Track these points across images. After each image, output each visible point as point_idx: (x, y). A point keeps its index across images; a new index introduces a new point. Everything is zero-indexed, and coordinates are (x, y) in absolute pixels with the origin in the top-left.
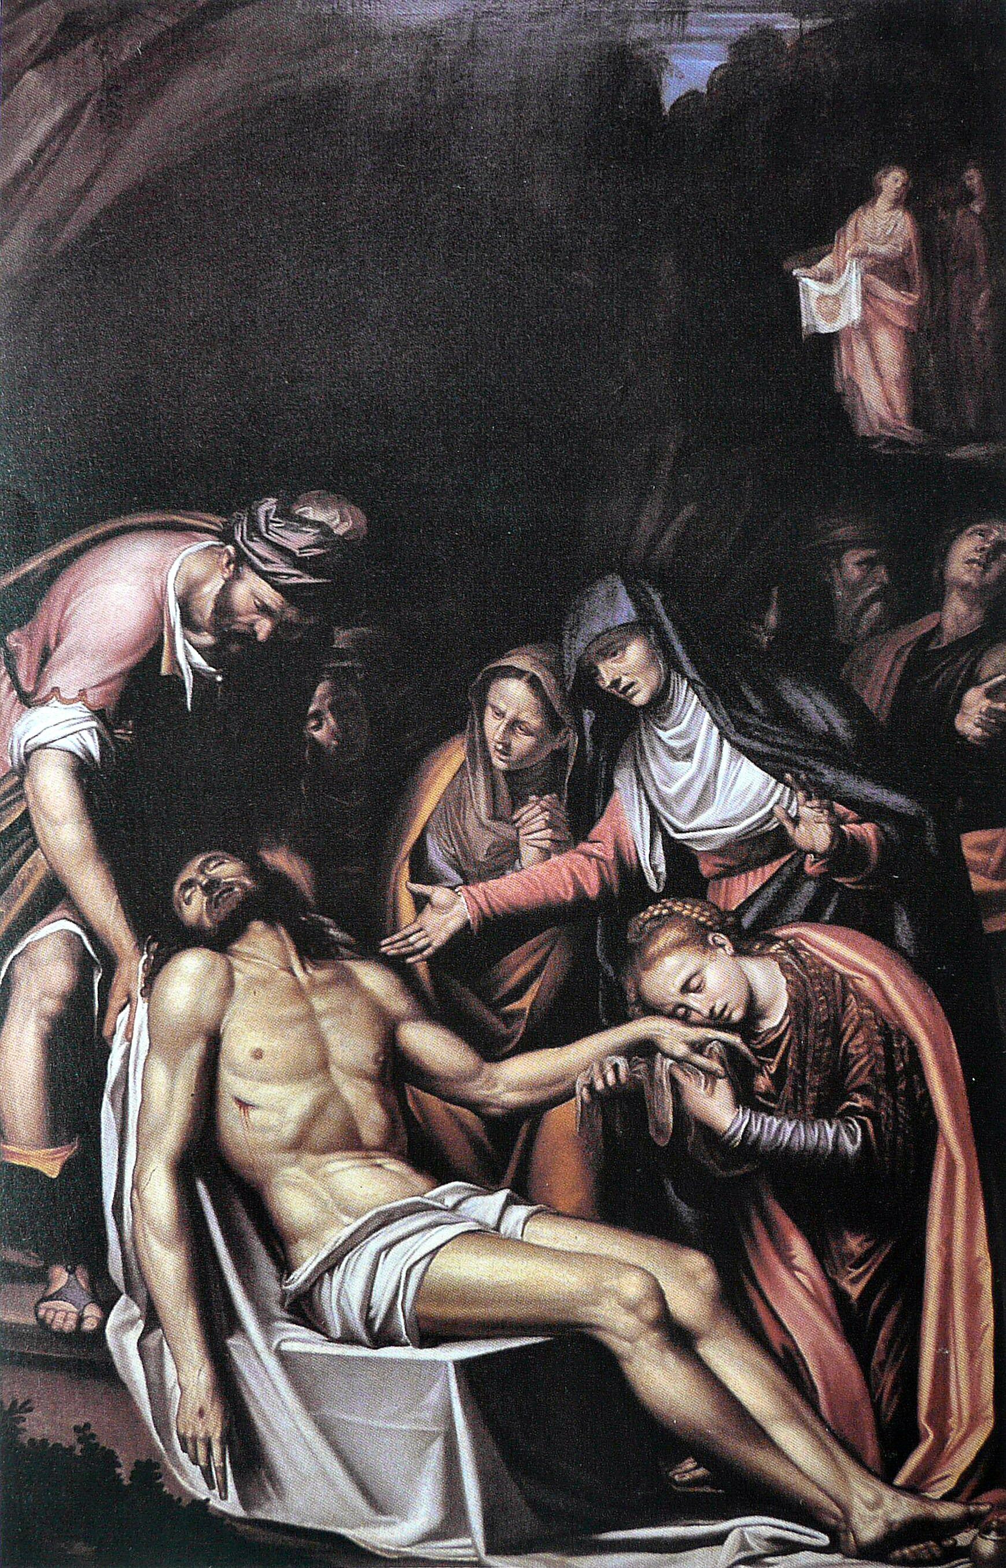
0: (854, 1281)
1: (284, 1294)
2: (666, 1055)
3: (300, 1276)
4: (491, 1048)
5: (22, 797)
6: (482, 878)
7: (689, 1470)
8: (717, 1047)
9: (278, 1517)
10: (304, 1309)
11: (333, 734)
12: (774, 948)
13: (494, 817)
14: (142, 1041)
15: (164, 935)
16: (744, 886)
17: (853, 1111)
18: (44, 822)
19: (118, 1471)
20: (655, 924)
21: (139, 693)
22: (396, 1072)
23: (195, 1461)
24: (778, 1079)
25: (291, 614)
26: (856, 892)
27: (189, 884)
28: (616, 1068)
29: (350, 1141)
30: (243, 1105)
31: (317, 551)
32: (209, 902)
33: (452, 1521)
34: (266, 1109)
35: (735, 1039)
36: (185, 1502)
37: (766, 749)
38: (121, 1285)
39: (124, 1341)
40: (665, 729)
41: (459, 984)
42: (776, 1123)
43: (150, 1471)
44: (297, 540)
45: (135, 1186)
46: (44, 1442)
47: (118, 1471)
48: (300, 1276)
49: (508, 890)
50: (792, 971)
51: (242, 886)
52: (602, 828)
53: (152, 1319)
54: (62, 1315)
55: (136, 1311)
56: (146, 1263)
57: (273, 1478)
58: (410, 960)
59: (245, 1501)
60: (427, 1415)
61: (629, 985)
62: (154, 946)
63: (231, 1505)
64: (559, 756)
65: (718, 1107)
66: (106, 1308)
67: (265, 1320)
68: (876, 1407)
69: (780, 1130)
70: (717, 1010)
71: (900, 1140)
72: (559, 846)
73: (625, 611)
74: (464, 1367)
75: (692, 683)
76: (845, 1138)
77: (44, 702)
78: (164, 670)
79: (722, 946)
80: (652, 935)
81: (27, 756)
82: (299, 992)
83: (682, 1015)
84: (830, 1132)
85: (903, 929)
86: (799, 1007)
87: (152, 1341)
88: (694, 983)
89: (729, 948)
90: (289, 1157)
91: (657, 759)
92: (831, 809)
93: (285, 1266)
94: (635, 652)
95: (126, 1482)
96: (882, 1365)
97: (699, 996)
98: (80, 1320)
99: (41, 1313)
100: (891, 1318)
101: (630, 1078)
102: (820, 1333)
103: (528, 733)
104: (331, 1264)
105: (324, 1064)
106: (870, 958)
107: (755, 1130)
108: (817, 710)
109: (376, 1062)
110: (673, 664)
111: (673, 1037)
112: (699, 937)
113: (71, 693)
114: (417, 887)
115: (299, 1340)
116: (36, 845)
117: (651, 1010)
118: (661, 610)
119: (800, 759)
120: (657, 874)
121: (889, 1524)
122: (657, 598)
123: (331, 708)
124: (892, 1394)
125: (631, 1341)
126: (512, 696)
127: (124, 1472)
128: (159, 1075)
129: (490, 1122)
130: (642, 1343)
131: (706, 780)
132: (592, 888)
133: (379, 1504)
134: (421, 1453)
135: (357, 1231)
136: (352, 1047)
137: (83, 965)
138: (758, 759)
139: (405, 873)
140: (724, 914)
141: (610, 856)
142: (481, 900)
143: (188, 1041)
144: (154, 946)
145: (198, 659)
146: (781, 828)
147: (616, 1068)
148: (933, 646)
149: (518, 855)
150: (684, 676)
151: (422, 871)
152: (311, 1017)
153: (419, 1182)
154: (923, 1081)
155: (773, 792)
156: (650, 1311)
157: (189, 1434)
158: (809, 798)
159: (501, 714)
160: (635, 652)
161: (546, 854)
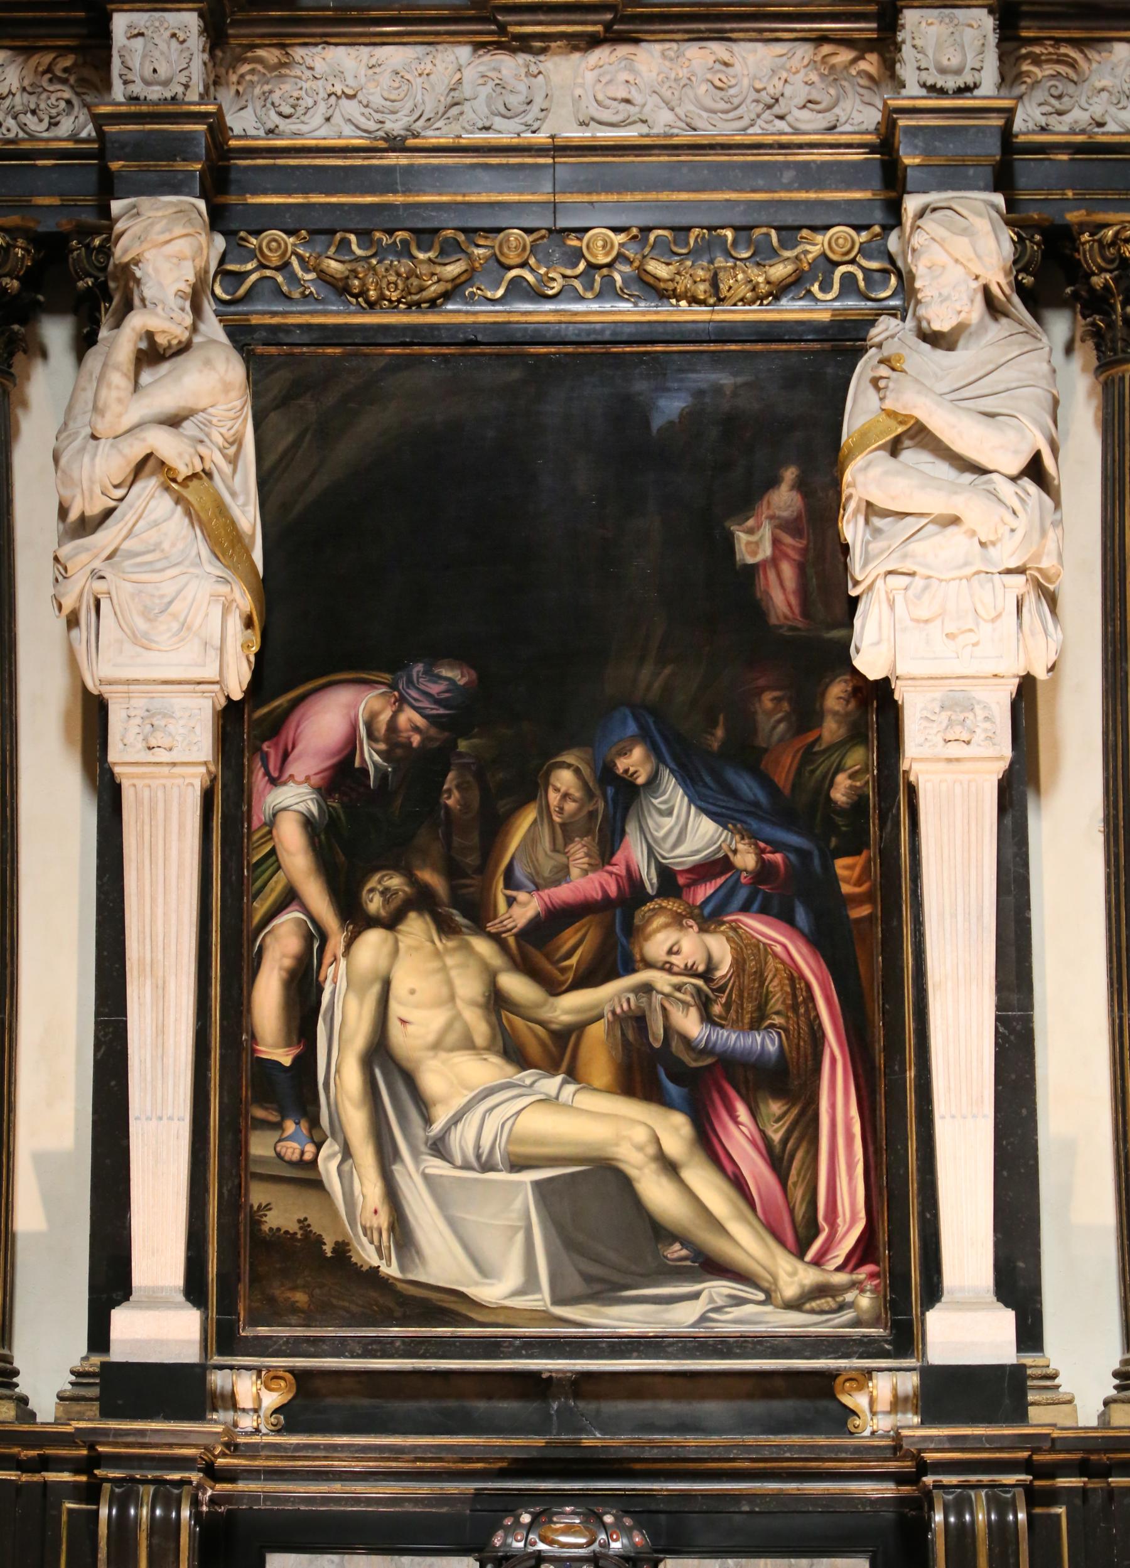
0: (776, 1131)
1: (427, 1138)
2: (658, 992)
3: (437, 1128)
4: (554, 989)
5: (272, 838)
6: (547, 886)
7: (676, 1251)
8: (689, 988)
9: (422, 1278)
10: (439, 1148)
11: (458, 802)
12: (723, 928)
13: (555, 850)
14: (342, 984)
15: (356, 919)
16: (704, 892)
17: (772, 1026)
18: (285, 854)
19: (324, 1247)
20: (651, 914)
21: (341, 776)
22: (496, 1002)
23: (372, 1242)
24: (727, 1006)
25: (433, 732)
26: (771, 894)
27: (372, 890)
28: (628, 1000)
29: (468, 1044)
30: (404, 1022)
31: (447, 695)
32: (384, 901)
33: (530, 1284)
34: (418, 1025)
35: (700, 982)
36: (364, 1269)
37: (719, 810)
38: (328, 1133)
39: (329, 1167)
40: (656, 798)
41: (533, 949)
42: (726, 1034)
43: (342, 1249)
44: (435, 689)
45: (338, 1071)
46: (279, 1229)
47: (324, 1247)
48: (437, 1128)
49: (563, 893)
50: (734, 942)
51: (404, 891)
52: (619, 857)
53: (347, 1153)
54: (292, 1150)
55: (336, 1148)
56: (343, 1118)
57: (419, 1252)
58: (504, 935)
59: (402, 1268)
60: (514, 1215)
61: (636, 951)
62: (351, 927)
63: (391, 1270)
64: (592, 815)
65: (690, 1024)
66: (319, 1146)
67: (416, 1154)
68: (791, 1211)
69: (730, 1038)
70: (689, 965)
71: (802, 1044)
72: (593, 867)
73: (632, 728)
74: (538, 1185)
75: (672, 771)
76: (768, 1041)
77: (285, 783)
78: (357, 764)
79: (691, 927)
80: (649, 921)
81: (275, 815)
82: (437, 954)
83: (667, 968)
84: (759, 1039)
85: (801, 916)
86: (739, 964)
87: (346, 1167)
88: (675, 949)
89: (696, 928)
90: (431, 1054)
91: (651, 815)
92: (757, 845)
93: (428, 1121)
94: (638, 753)
95: (329, 1255)
96: (795, 1184)
97: (678, 957)
98: (302, 1153)
99: (278, 1149)
100: (799, 1155)
101: (638, 1007)
102: (754, 1164)
103: (574, 801)
104: (456, 1120)
105: (452, 997)
106: (784, 935)
107: (713, 1038)
108: (747, 786)
109: (484, 996)
110: (660, 759)
111: (662, 981)
112: (678, 921)
113: (300, 777)
114: (509, 892)
115: (436, 1167)
116: (279, 867)
117: (649, 965)
118: (653, 727)
119: (737, 815)
120: (652, 885)
121: (802, 1286)
122: (651, 721)
123: (458, 787)
124: (801, 1203)
125: (640, 1168)
126: (565, 779)
127: (328, 1249)
128: (353, 1004)
129: (554, 1034)
130: (646, 1171)
131: (682, 829)
132: (613, 891)
133: (484, 1271)
134: (511, 1239)
135: (474, 1097)
136: (469, 987)
137: (308, 938)
138: (714, 816)
139: (501, 885)
140: (692, 907)
141: (624, 873)
142: (546, 899)
143: (371, 983)
144: (351, 927)
145: (376, 757)
146: (726, 857)
147: (628, 1000)
148: (816, 749)
149: (568, 873)
150: (667, 766)
151: (510, 882)
152: (444, 969)
153: (509, 1069)
154: (815, 1008)
155: (720, 836)
156: (651, 1150)
157: (368, 1225)
158: (743, 838)
159: (557, 790)
160: (638, 753)
161: (585, 872)
